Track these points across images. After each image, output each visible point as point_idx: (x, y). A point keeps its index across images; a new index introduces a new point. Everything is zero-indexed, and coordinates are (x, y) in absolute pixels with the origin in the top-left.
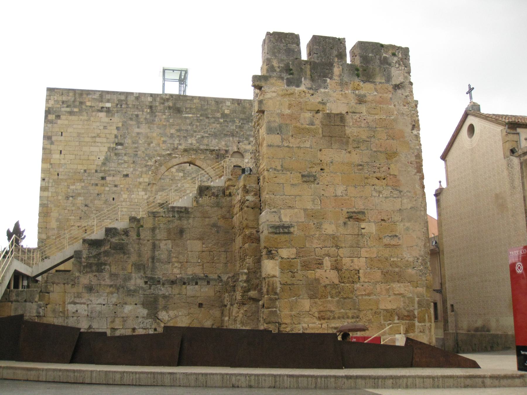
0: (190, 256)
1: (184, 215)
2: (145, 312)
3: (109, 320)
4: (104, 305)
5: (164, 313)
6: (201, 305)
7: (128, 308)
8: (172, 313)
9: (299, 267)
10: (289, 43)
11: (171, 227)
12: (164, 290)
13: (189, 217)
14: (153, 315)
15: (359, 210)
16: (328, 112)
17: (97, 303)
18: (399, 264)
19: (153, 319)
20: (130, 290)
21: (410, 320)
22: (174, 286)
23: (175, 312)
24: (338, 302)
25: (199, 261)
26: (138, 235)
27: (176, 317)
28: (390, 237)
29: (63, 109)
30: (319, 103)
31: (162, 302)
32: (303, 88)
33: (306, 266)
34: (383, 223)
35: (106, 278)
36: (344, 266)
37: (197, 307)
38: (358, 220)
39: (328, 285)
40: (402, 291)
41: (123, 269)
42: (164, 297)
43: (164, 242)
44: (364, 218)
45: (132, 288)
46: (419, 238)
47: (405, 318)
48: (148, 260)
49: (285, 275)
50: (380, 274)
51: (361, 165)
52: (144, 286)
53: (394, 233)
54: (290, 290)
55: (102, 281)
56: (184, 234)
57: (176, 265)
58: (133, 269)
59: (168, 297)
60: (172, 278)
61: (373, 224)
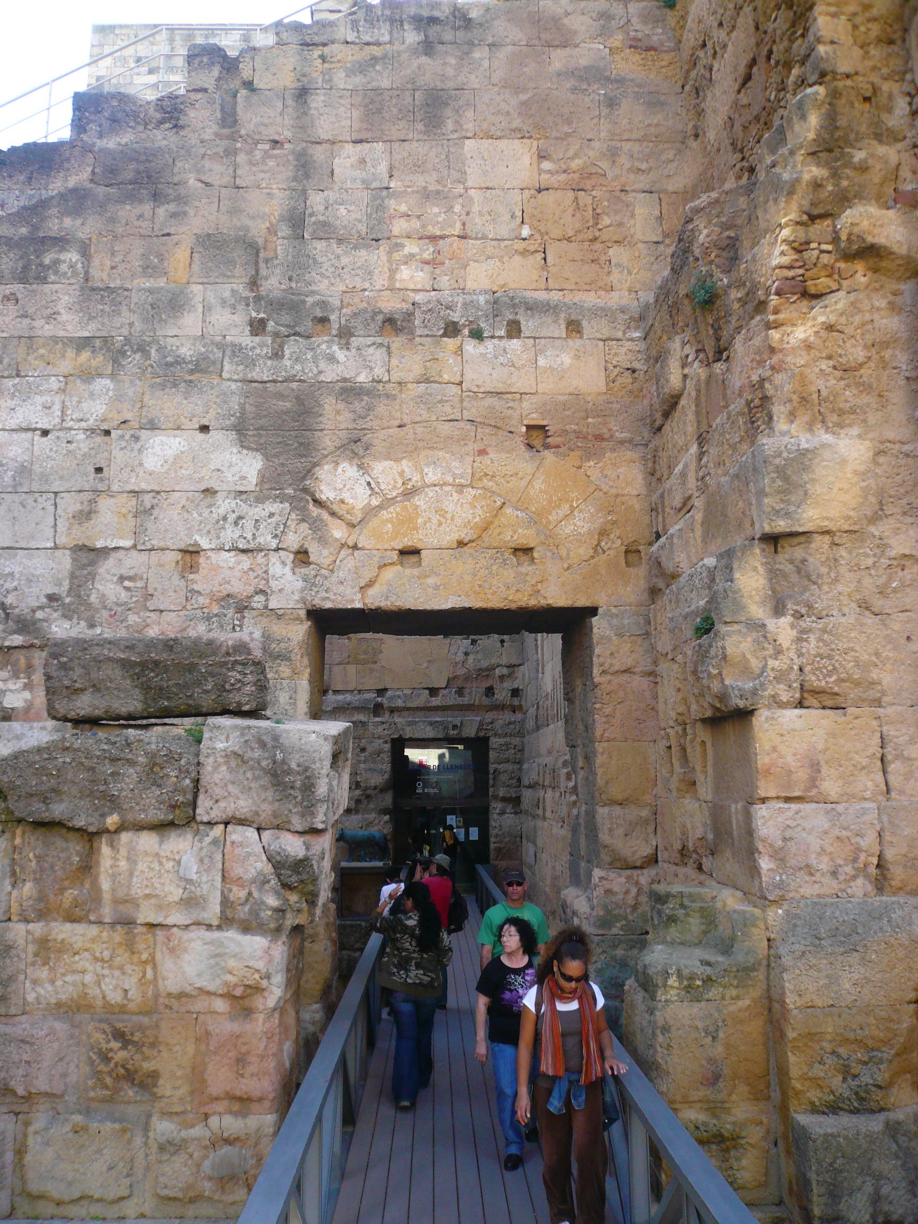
0: (475, 209)
1: (448, 36)
2: (249, 467)
3: (70, 504)
4: (45, 433)
5: (347, 470)
6: (537, 435)
7: (162, 450)
8: (387, 473)
11: (385, 83)
12: (343, 363)
13: (471, 44)
14: (292, 479)
17: (13, 423)
19: (291, 499)
20: (179, 361)
22: (397, 342)
23: (406, 465)
25: (526, 232)
26: (229, 119)
27: (410, 493)
29: (138, 80)
31: (334, 418)
35: (61, 308)
37: (518, 442)
41: (148, 270)
42: (349, 391)
43: (349, 148)
45: (186, 351)
48: (272, 231)
52: (247, 340)
55: (38, 323)
56: (448, 112)
57: (411, 248)
58: (196, 267)
59: (369, 393)
60: (390, 304)
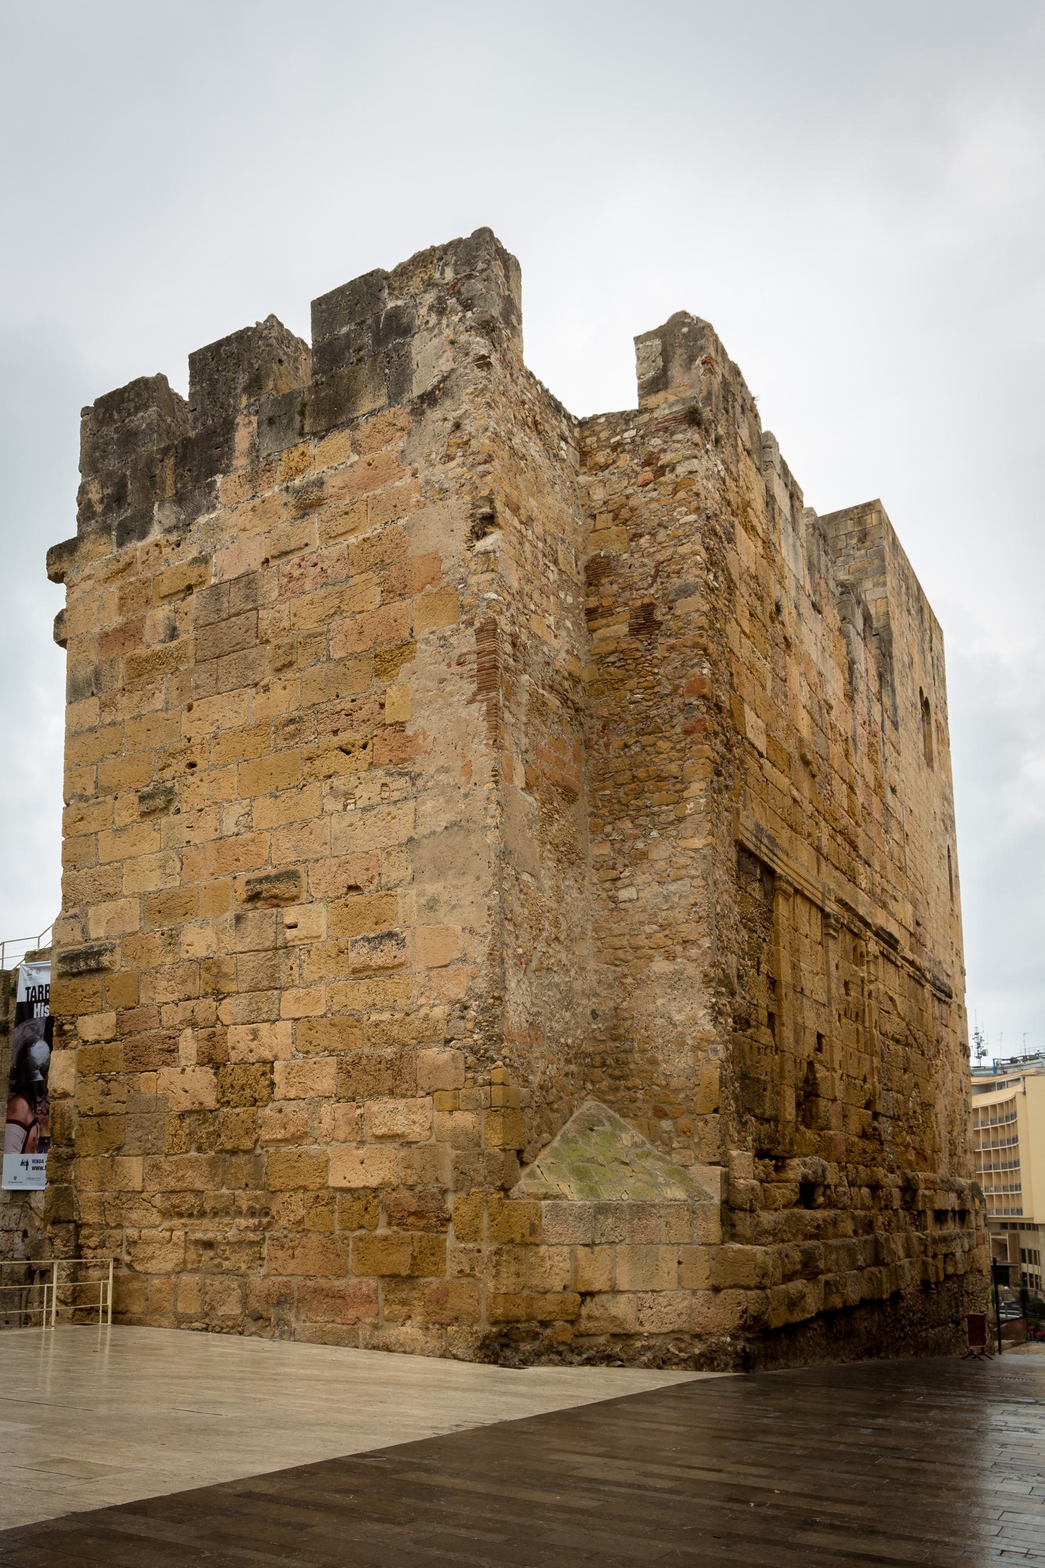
9: (121, 1065)
10: (129, 415)
15: (282, 869)
16: (214, 580)
18: (395, 1031)
21: (426, 1229)
24: (212, 1164)
28: (369, 940)
30: (195, 560)
32: (156, 534)
33: (138, 1060)
34: (354, 898)
36: (232, 1053)
38: (277, 901)
39: (191, 1112)
40: (400, 1125)
44: (294, 891)
46: (472, 931)
47: (411, 1220)
49: (90, 1088)
50: (332, 1070)
51: (292, 721)
53: (384, 928)
54: (100, 1130)
61: (320, 907)
